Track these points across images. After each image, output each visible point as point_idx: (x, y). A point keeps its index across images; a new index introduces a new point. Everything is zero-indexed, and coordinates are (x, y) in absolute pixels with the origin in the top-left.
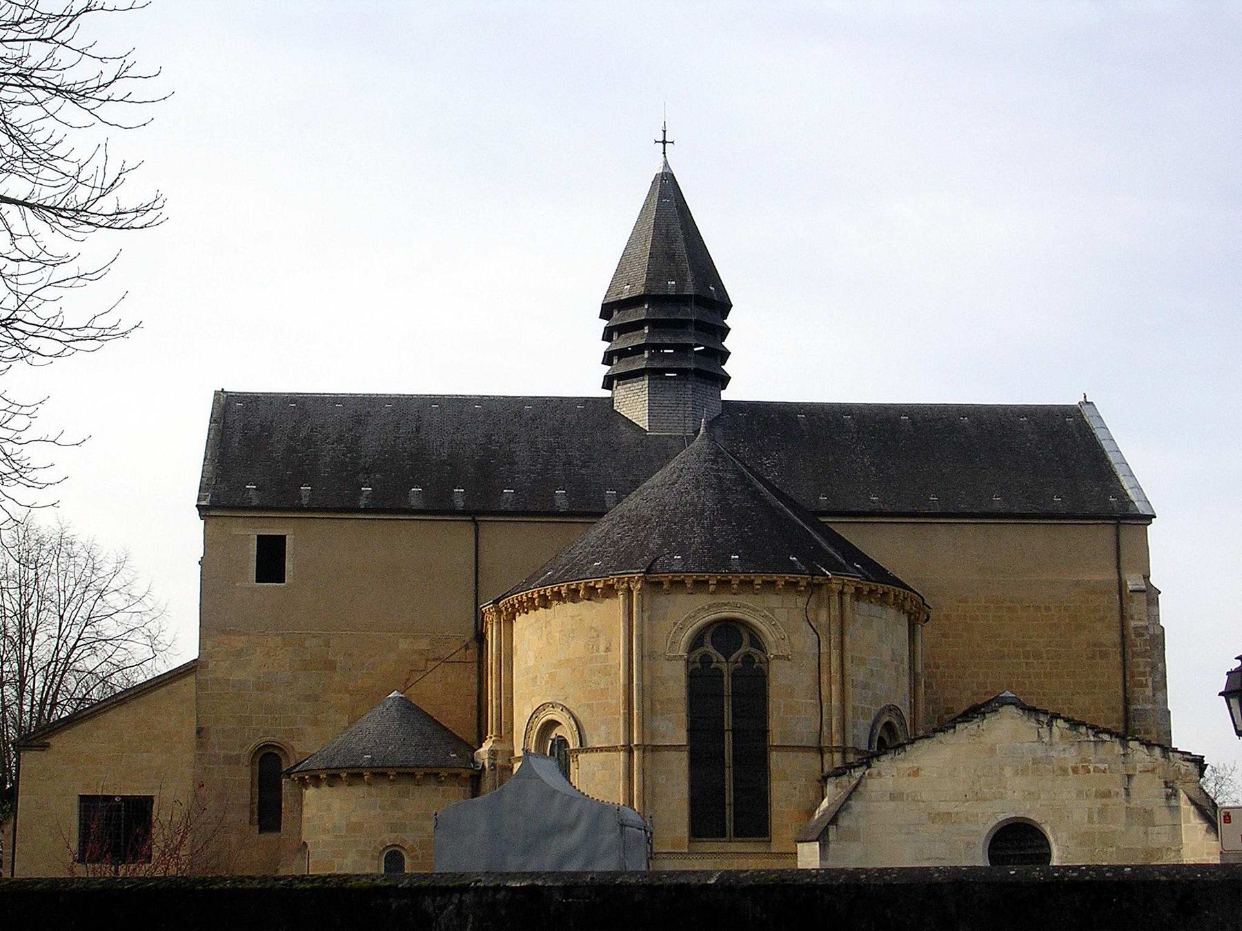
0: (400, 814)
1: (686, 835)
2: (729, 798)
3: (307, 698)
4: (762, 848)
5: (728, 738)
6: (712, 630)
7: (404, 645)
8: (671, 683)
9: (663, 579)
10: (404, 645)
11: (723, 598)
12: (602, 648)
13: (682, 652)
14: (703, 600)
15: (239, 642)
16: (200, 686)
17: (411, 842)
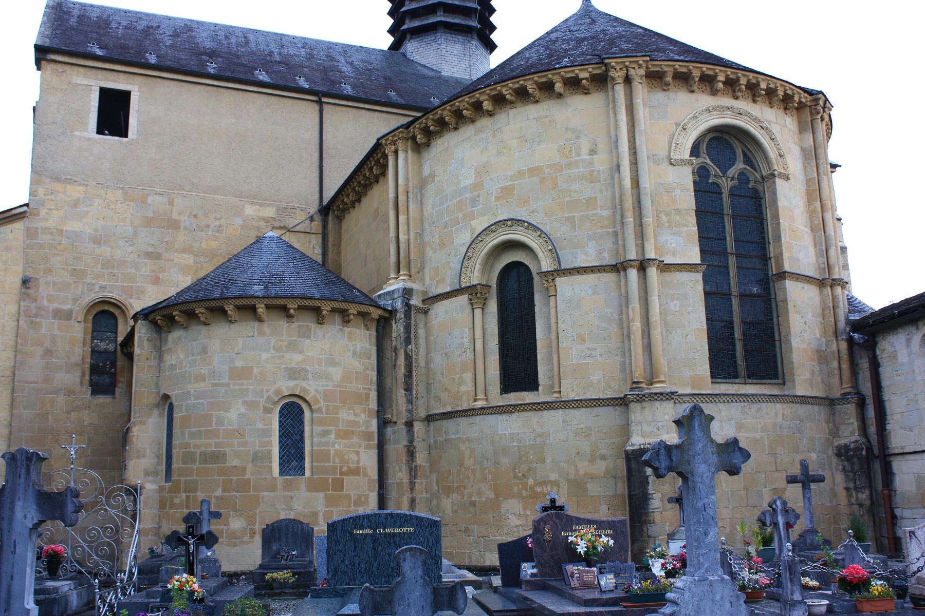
0: (298, 357)
1: (709, 373)
2: (738, 334)
3: (148, 255)
4: (775, 391)
5: (732, 262)
6: (707, 140)
7: (250, 210)
8: (678, 192)
9: (666, 69)
10: (250, 210)
11: (726, 101)
12: (585, 149)
13: (687, 156)
14: (703, 100)
15: (75, 192)
16: (31, 234)
17: (313, 393)
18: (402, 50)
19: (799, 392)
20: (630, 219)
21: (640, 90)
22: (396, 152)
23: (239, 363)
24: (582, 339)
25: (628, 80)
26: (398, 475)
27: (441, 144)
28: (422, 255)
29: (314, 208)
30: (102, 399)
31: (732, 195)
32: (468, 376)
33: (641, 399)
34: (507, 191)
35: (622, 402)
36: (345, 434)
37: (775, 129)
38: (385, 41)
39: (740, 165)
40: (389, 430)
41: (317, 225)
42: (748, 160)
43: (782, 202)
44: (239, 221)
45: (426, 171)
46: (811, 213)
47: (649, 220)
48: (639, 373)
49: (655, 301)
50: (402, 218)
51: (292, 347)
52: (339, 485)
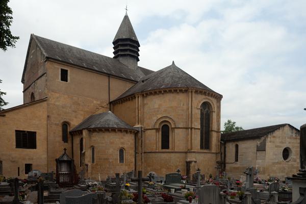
3: (74, 111)
10: (95, 102)
11: (207, 97)
12: (182, 104)
14: (203, 96)
15: (57, 95)
16: (48, 105)
18: (118, 59)
19: (213, 152)
20: (190, 119)
21: (193, 94)
22: (138, 97)
23: (112, 141)
24: (179, 141)
25: (192, 92)
26: (139, 163)
27: (150, 98)
28: (143, 119)
29: (108, 102)
30: (66, 144)
31: (206, 115)
32: (155, 146)
33: (190, 152)
34: (165, 111)
35: (186, 153)
36: (130, 155)
37: (214, 102)
38: (112, 56)
39: (207, 109)
40: (137, 155)
41: (109, 106)
42: (208, 108)
43: (213, 117)
44: (92, 104)
45: (145, 102)
46: (217, 118)
47: (193, 120)
48: (189, 148)
49: (193, 135)
50: (140, 112)
51: (122, 138)
52: (129, 165)
